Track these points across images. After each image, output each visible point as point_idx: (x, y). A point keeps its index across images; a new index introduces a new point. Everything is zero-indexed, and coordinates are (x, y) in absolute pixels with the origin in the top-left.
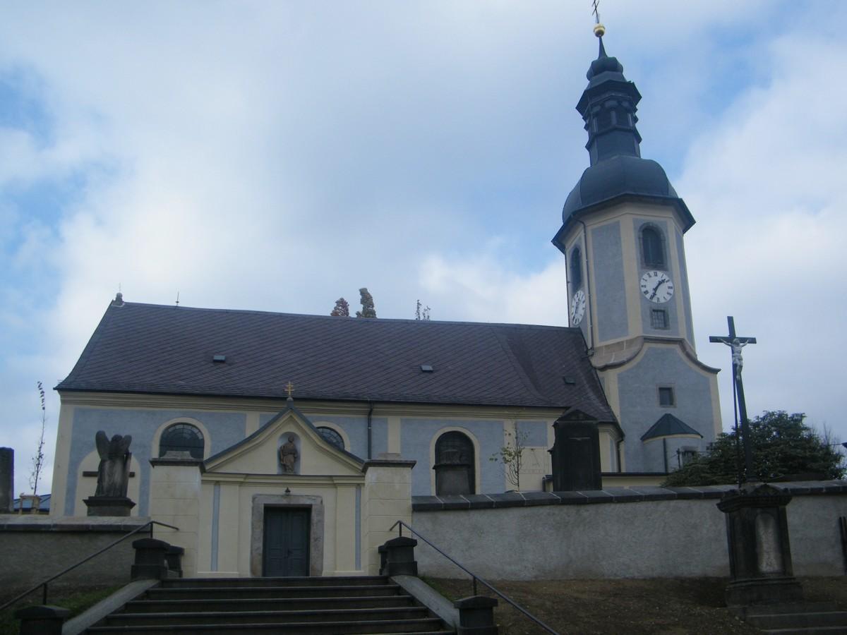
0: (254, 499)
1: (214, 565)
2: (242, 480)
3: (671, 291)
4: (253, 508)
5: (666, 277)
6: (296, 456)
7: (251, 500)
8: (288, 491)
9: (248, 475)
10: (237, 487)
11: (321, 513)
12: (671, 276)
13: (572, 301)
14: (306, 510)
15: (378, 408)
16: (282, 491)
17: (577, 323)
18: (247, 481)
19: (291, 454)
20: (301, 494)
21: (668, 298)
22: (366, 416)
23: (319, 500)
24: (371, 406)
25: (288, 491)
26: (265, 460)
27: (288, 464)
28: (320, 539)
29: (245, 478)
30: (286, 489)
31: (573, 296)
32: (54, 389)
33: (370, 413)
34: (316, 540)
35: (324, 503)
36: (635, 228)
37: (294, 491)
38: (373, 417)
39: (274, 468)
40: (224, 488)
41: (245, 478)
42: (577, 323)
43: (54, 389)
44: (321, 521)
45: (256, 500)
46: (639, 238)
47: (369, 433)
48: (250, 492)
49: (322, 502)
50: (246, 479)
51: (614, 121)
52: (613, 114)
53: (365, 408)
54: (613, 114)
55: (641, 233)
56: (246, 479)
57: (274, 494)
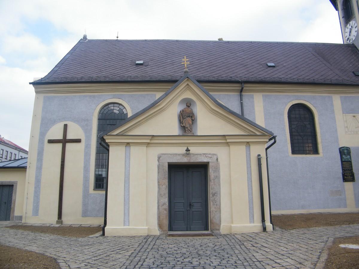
0: (159, 158)
1: (126, 221)
2: (148, 141)
6: (193, 119)
7: (157, 158)
8: (188, 150)
9: (153, 136)
10: (144, 148)
11: (217, 169)
13: (345, 30)
14: (203, 168)
15: (247, 87)
16: (182, 150)
17: (351, 41)
18: (152, 142)
19: (189, 116)
20: (199, 153)
22: (239, 93)
23: (215, 157)
24: (242, 85)
25: (188, 150)
26: (167, 122)
27: (188, 126)
28: (217, 194)
29: (151, 140)
30: (186, 148)
31: (346, 26)
32: (30, 83)
33: (241, 91)
34: (214, 195)
35: (219, 160)
37: (193, 150)
38: (243, 93)
39: (175, 130)
40: (134, 150)
41: (151, 140)
42: (351, 41)
43: (30, 83)
44: (218, 177)
45: (161, 159)
47: (242, 104)
48: (155, 152)
49: (217, 159)
50: (152, 140)
53: (237, 87)
56: (152, 140)
57: (176, 153)
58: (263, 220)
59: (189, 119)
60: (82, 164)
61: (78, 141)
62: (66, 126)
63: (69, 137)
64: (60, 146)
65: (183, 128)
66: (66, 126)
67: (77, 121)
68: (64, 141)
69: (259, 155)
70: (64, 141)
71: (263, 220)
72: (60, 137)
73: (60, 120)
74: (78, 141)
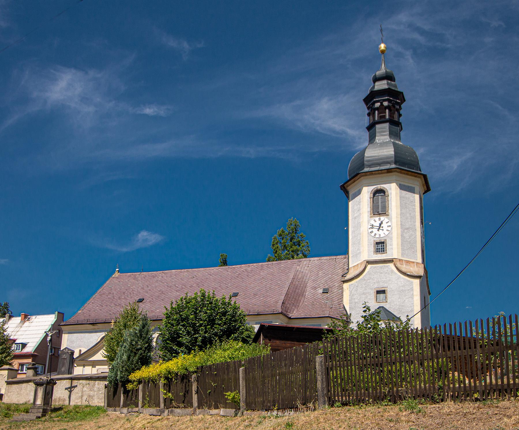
3: (389, 229)
5: (386, 220)
12: (390, 219)
21: (387, 233)
36: (368, 192)
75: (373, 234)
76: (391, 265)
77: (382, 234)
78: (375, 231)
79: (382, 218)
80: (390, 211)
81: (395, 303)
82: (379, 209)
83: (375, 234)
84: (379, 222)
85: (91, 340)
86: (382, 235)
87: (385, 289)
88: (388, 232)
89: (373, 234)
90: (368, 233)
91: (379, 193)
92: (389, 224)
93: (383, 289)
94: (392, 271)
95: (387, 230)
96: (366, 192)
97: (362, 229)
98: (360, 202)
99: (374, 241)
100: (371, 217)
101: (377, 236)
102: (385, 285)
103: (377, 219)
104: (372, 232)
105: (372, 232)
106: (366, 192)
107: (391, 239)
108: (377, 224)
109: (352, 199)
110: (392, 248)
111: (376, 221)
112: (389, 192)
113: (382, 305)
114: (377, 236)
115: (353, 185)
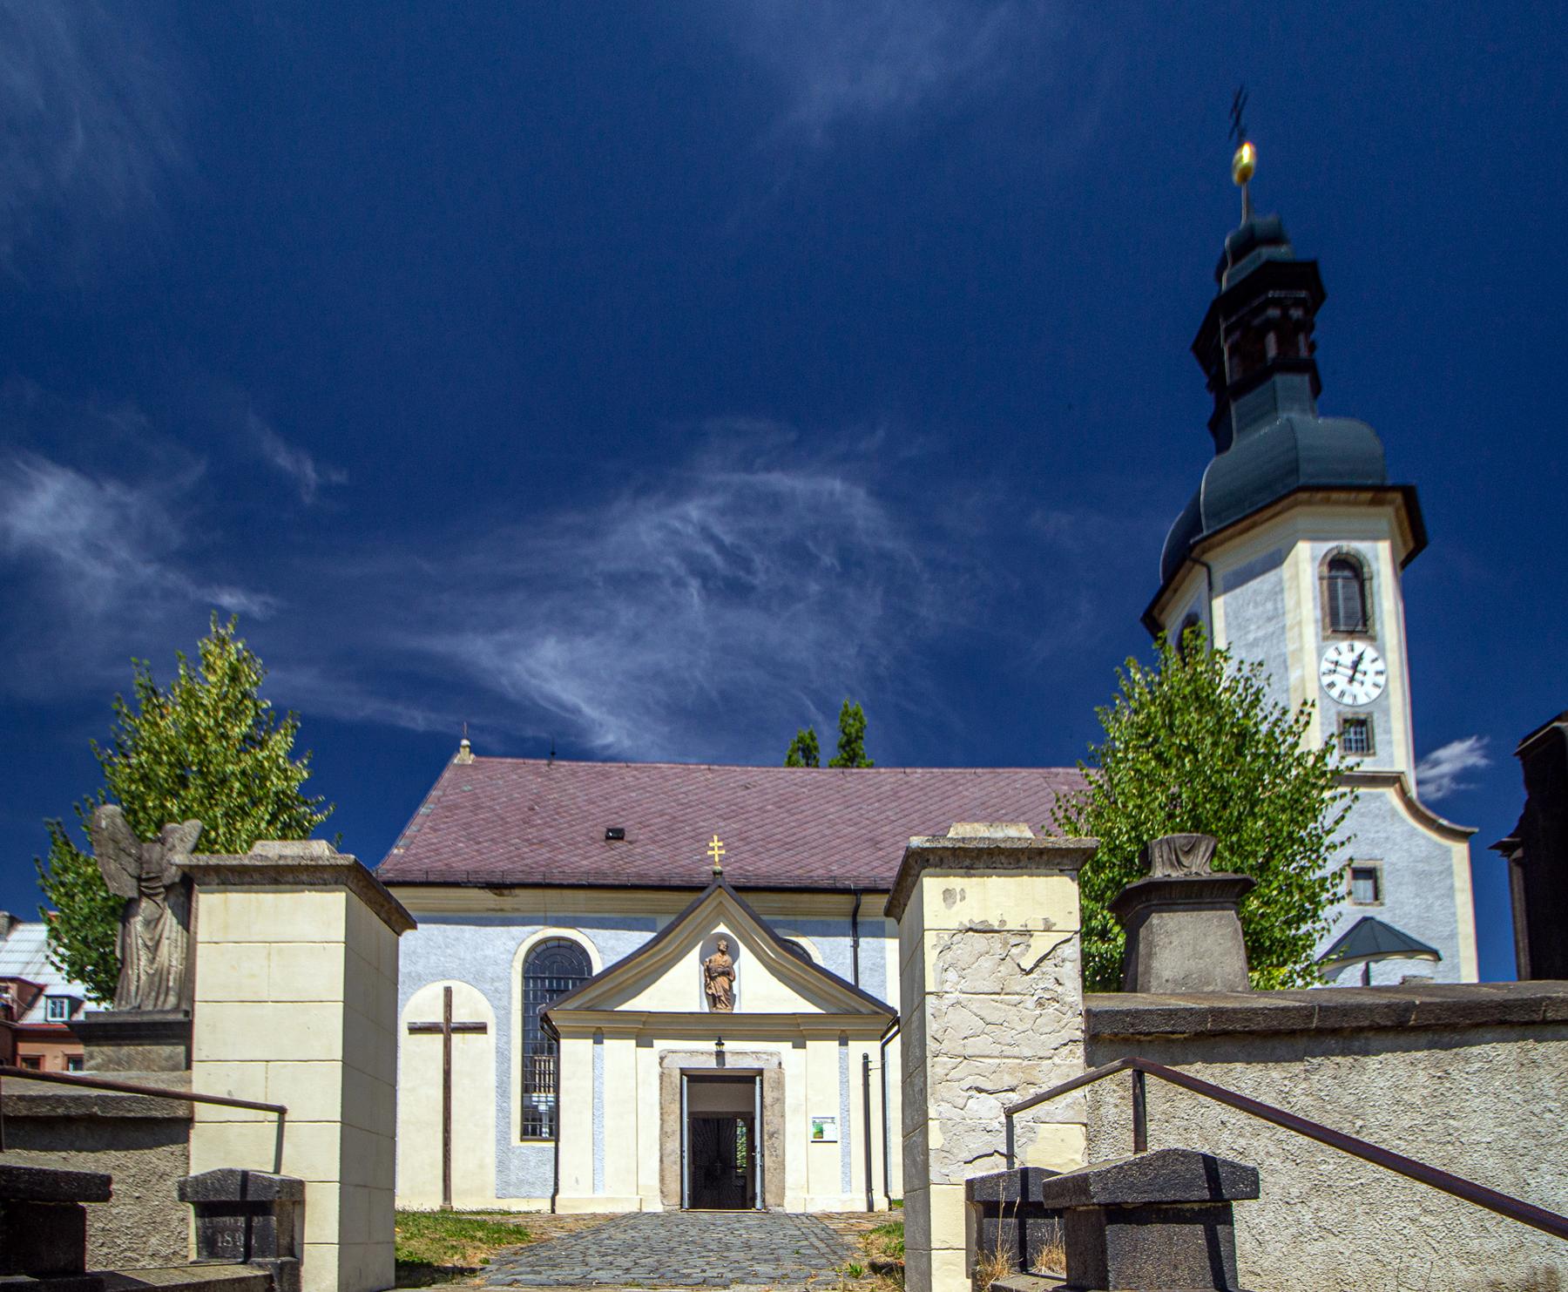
0: (662, 1059)
3: (1381, 680)
4: (662, 1076)
5: (1370, 653)
11: (780, 1084)
12: (1382, 652)
20: (742, 1053)
21: (1375, 693)
34: (771, 1136)
36: (1313, 559)
44: (780, 1100)
46: (1321, 578)
51: (1272, 352)
52: (1271, 339)
54: (1271, 339)
55: (1325, 569)
57: (699, 1053)
58: (869, 1189)
59: (723, 981)
60: (492, 1079)
61: (481, 1028)
62: (448, 992)
63: (459, 1017)
64: (440, 1038)
65: (714, 1000)
66: (448, 992)
67: (477, 980)
68: (447, 1029)
69: (866, 1057)
70: (447, 1029)
71: (869, 1189)
72: (439, 1018)
73: (435, 977)
74: (481, 1028)
75: (1335, 693)
76: (1390, 794)
77: (1363, 694)
78: (1341, 680)
79: (1360, 646)
80: (1378, 627)
81: (1406, 909)
82: (1348, 614)
83: (1342, 694)
84: (1354, 656)
85: (489, 952)
86: (1362, 700)
87: (1378, 864)
88: (1377, 692)
89: (1335, 693)
90: (1321, 687)
91: (1346, 571)
92: (1379, 665)
93: (1370, 864)
94: (1394, 813)
95: (1376, 685)
96: (1305, 562)
97: (1294, 675)
98: (1278, 591)
99: (1339, 714)
100: (1325, 638)
101: (1347, 700)
102: (1377, 852)
103: (1344, 645)
104: (1332, 685)
105: (1332, 685)
106: (1305, 562)
107: (1386, 712)
108: (1347, 658)
109: (1228, 589)
110: (1390, 743)
111: (1345, 650)
112: (1374, 567)
113: (1371, 911)
114: (1347, 700)
115: (1237, 541)
